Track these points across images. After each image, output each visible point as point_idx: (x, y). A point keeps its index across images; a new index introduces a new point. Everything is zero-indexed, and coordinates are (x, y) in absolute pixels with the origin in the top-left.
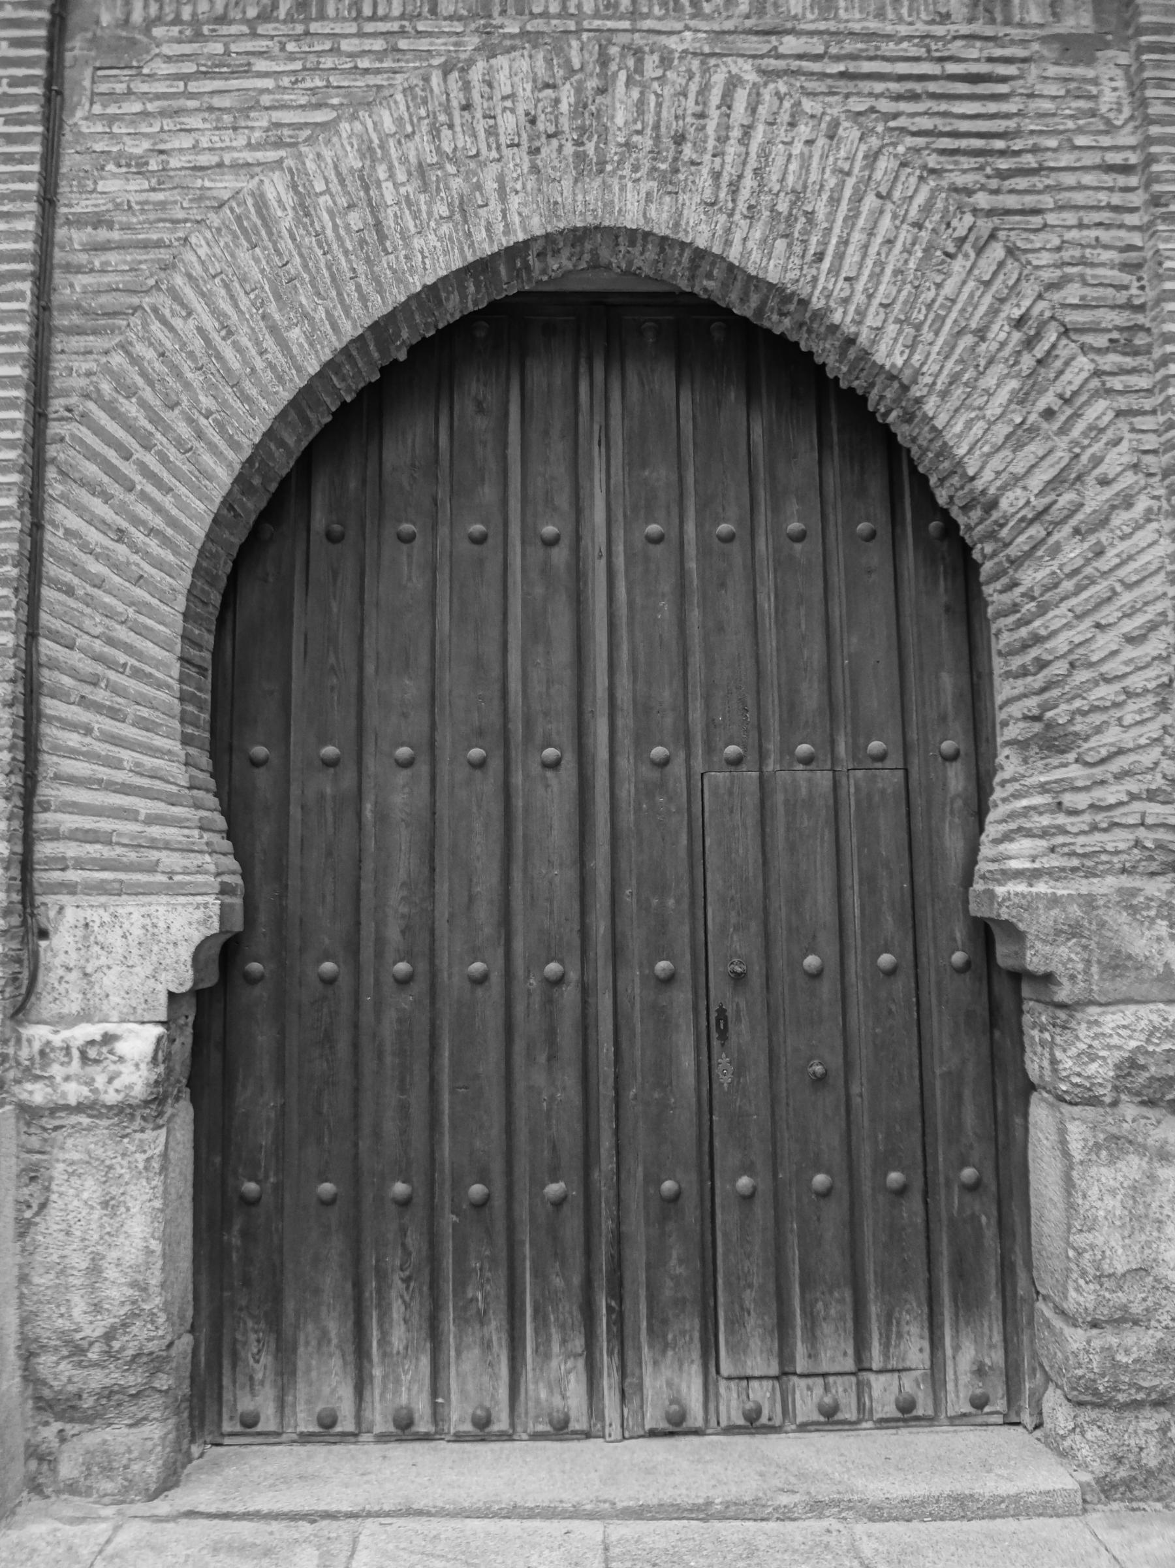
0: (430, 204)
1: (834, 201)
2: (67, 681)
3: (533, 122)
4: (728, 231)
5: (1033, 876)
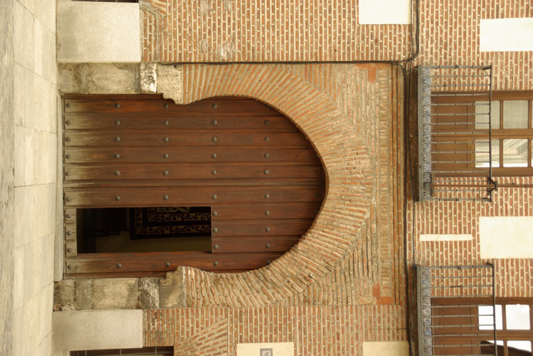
0: (334, 146)
1: (336, 235)
2: (229, 70)
3: (354, 168)
4: (328, 211)
5: (187, 275)
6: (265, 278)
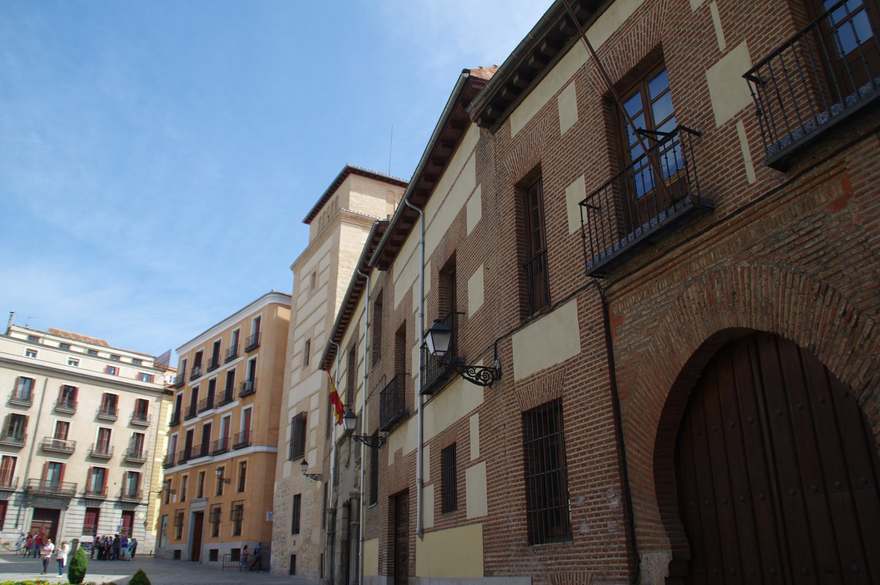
6: (866, 387)
